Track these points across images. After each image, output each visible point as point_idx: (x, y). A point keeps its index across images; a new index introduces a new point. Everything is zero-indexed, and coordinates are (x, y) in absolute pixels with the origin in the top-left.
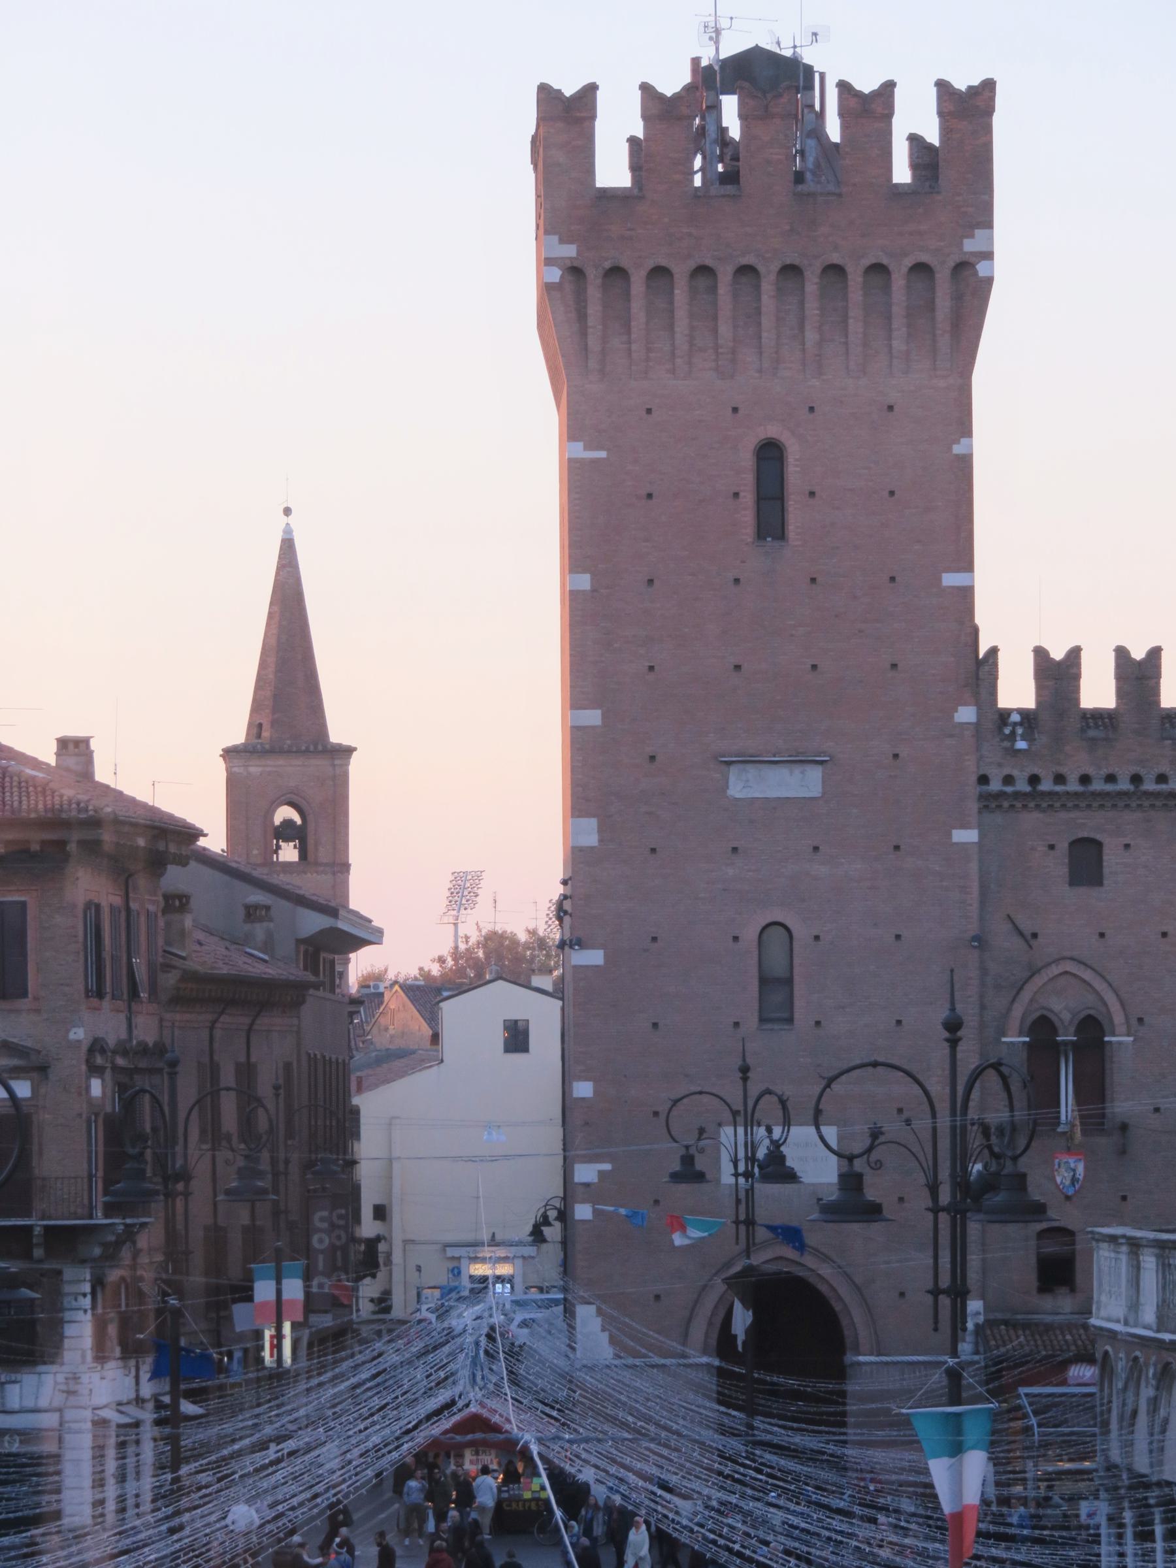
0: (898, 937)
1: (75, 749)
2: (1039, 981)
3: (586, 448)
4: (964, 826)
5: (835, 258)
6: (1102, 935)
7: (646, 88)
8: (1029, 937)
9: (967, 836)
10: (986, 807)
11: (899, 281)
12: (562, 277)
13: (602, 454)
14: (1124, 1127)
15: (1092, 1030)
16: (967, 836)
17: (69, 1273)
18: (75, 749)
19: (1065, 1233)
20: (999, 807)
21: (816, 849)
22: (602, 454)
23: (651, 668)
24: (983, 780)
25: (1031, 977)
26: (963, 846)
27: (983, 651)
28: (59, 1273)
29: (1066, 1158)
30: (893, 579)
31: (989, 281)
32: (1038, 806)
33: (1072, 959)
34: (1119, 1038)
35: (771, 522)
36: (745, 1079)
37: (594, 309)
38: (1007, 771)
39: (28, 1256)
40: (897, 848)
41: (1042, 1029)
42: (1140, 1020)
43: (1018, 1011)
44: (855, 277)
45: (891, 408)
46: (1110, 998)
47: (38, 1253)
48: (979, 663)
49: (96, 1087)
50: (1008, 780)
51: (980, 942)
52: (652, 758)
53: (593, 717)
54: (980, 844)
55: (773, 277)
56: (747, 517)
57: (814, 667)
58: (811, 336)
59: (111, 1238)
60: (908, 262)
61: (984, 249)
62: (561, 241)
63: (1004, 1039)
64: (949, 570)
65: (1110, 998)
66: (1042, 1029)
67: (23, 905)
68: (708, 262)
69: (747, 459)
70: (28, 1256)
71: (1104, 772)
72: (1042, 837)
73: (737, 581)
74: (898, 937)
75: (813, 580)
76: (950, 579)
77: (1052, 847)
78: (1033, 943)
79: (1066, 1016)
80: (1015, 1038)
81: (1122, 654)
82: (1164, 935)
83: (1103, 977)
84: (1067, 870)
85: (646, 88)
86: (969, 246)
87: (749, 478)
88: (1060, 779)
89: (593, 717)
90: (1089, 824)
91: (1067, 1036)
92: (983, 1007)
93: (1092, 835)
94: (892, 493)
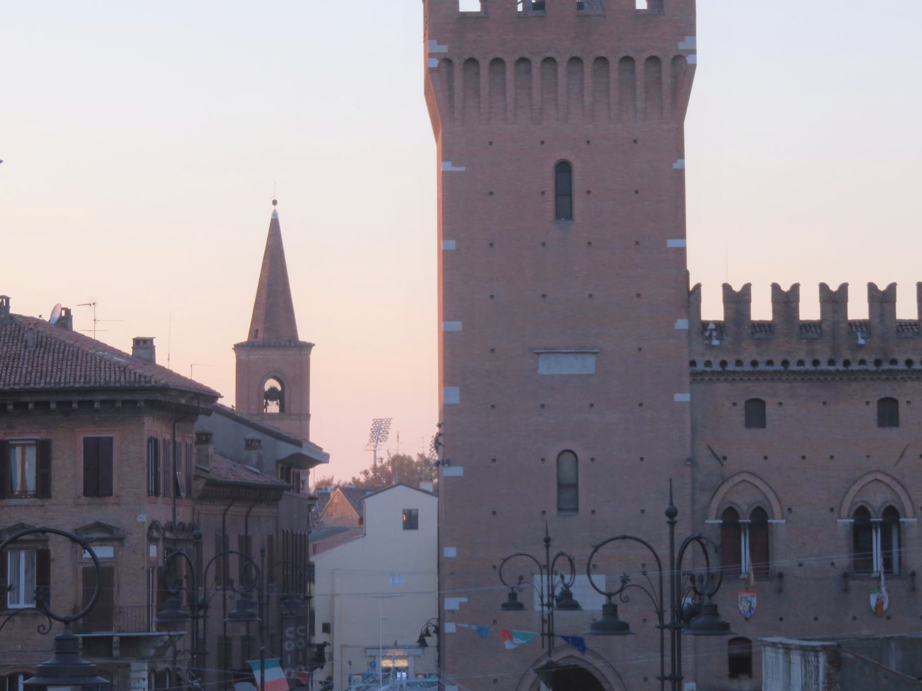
0: (642, 459)
1: (144, 345)
2: (727, 486)
3: (453, 165)
4: (681, 391)
5: (602, 53)
6: (766, 458)
8: (721, 459)
9: (683, 397)
10: (695, 380)
11: (640, 67)
12: (439, 64)
13: (462, 169)
14: (781, 576)
15: (760, 516)
17: (135, 665)
18: (144, 345)
19: (745, 641)
20: (702, 380)
21: (592, 405)
22: (462, 169)
23: (492, 296)
24: (693, 363)
25: (723, 483)
27: (692, 286)
28: (129, 666)
29: (745, 594)
30: (637, 243)
31: (694, 66)
32: (726, 380)
33: (747, 472)
34: (777, 521)
35: (564, 208)
36: (548, 546)
37: (458, 83)
38: (706, 358)
39: (110, 655)
40: (641, 405)
41: (730, 514)
42: (790, 510)
43: (715, 504)
44: (614, 64)
45: (635, 141)
46: (771, 496)
47: (116, 653)
48: (690, 293)
49: (153, 551)
50: (708, 363)
51: (692, 461)
52: (493, 351)
53: (457, 326)
54: (691, 403)
55: (565, 64)
56: (549, 204)
57: (590, 296)
59: (160, 644)
60: (646, 55)
61: (690, 48)
62: (439, 43)
63: (707, 521)
64: (671, 238)
65: (771, 496)
66: (730, 514)
67: (111, 439)
68: (527, 55)
69: (549, 171)
70: (110, 655)
71: (766, 359)
72: (729, 398)
73: (544, 244)
74: (642, 459)
75: (590, 244)
76: (672, 243)
77: (735, 404)
78: (724, 462)
79: (745, 507)
80: (714, 521)
81: (775, 287)
82: (803, 457)
83: (766, 483)
84: (744, 418)
86: (682, 46)
88: (739, 363)
89: (457, 326)
90: (758, 390)
91: (745, 520)
92: (694, 502)
93: (758, 397)
94: (637, 192)
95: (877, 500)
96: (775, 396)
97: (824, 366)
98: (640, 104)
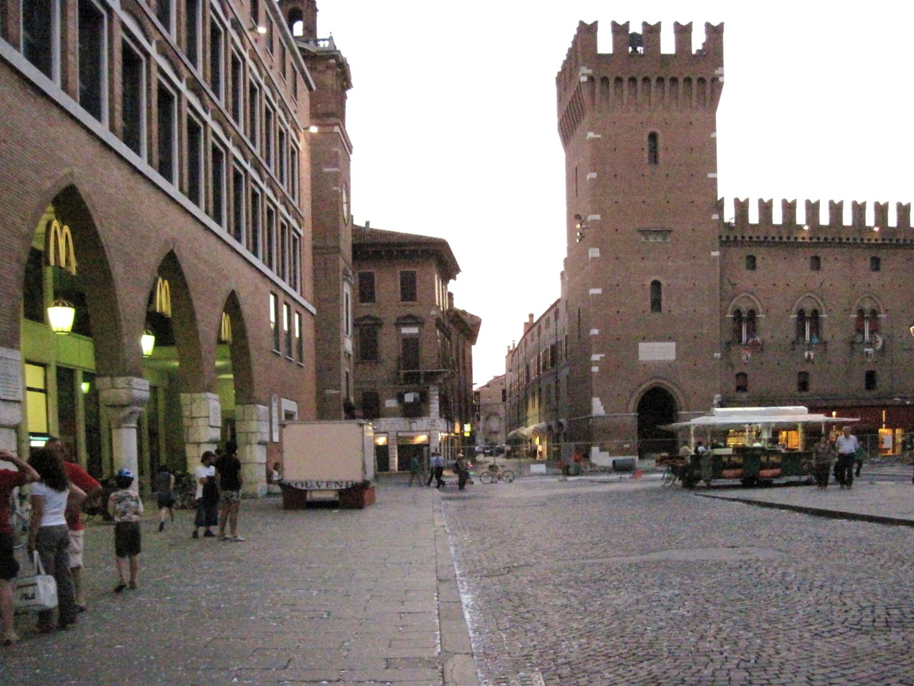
9: (716, 254)
13: (599, 136)
15: (752, 313)
16: (716, 254)
17: (431, 388)
22: (599, 136)
27: (719, 198)
31: (723, 83)
34: (761, 316)
37: (597, 91)
41: (738, 313)
43: (730, 308)
46: (758, 303)
47: (422, 381)
58: (666, 100)
59: (446, 376)
66: (738, 313)
70: (418, 382)
76: (710, 176)
80: (730, 316)
86: (717, 72)
88: (743, 237)
90: (753, 251)
91: (745, 316)
95: (809, 307)
96: (760, 254)
97: (785, 239)
98: (694, 104)
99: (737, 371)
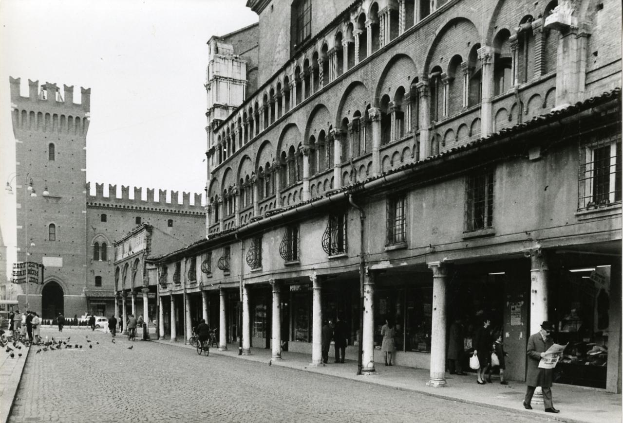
7: (29, 80)
15: (105, 245)
26: (84, 213)
27: (87, 182)
41: (96, 244)
62: (15, 104)
66: (96, 244)
76: (83, 170)
85: (29, 80)
87: (48, 149)
91: (100, 245)
96: (108, 213)
99: (96, 275)
